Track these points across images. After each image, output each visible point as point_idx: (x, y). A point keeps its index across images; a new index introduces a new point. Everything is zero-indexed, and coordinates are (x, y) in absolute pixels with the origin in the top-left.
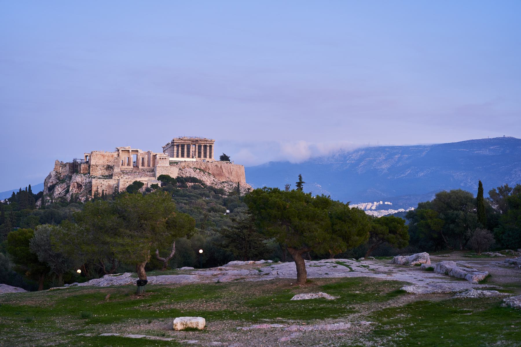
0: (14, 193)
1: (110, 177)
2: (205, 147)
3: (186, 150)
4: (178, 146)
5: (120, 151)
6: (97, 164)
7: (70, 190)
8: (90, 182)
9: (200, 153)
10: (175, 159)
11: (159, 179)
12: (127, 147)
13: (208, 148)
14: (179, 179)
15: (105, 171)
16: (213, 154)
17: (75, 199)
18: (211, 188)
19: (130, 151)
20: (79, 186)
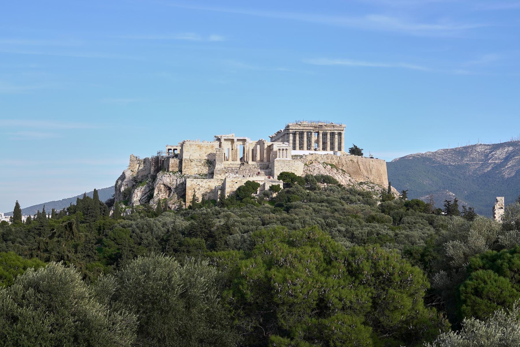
0: (78, 199)
2: (333, 134)
3: (305, 139)
4: (294, 134)
6: (191, 158)
7: (155, 195)
8: (184, 184)
9: (324, 143)
10: (298, 152)
12: (231, 135)
13: (336, 136)
15: (203, 167)
16: (343, 145)
17: (163, 207)
18: (352, 191)
19: (235, 140)
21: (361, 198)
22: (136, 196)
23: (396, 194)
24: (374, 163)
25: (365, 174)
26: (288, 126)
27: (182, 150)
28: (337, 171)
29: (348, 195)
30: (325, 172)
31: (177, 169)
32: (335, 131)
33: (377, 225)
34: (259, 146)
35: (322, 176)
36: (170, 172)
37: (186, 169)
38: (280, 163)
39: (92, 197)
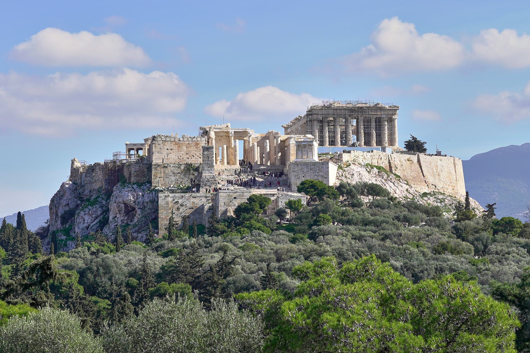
5: (212, 135)
7: (111, 218)
11: (299, 191)
20: (129, 210)
21: (424, 216)
22: (81, 220)
23: (478, 208)
25: (430, 179)
27: (150, 151)
29: (406, 213)
30: (370, 178)
33: (450, 257)
34: (268, 141)
38: (300, 167)
39: (15, 225)
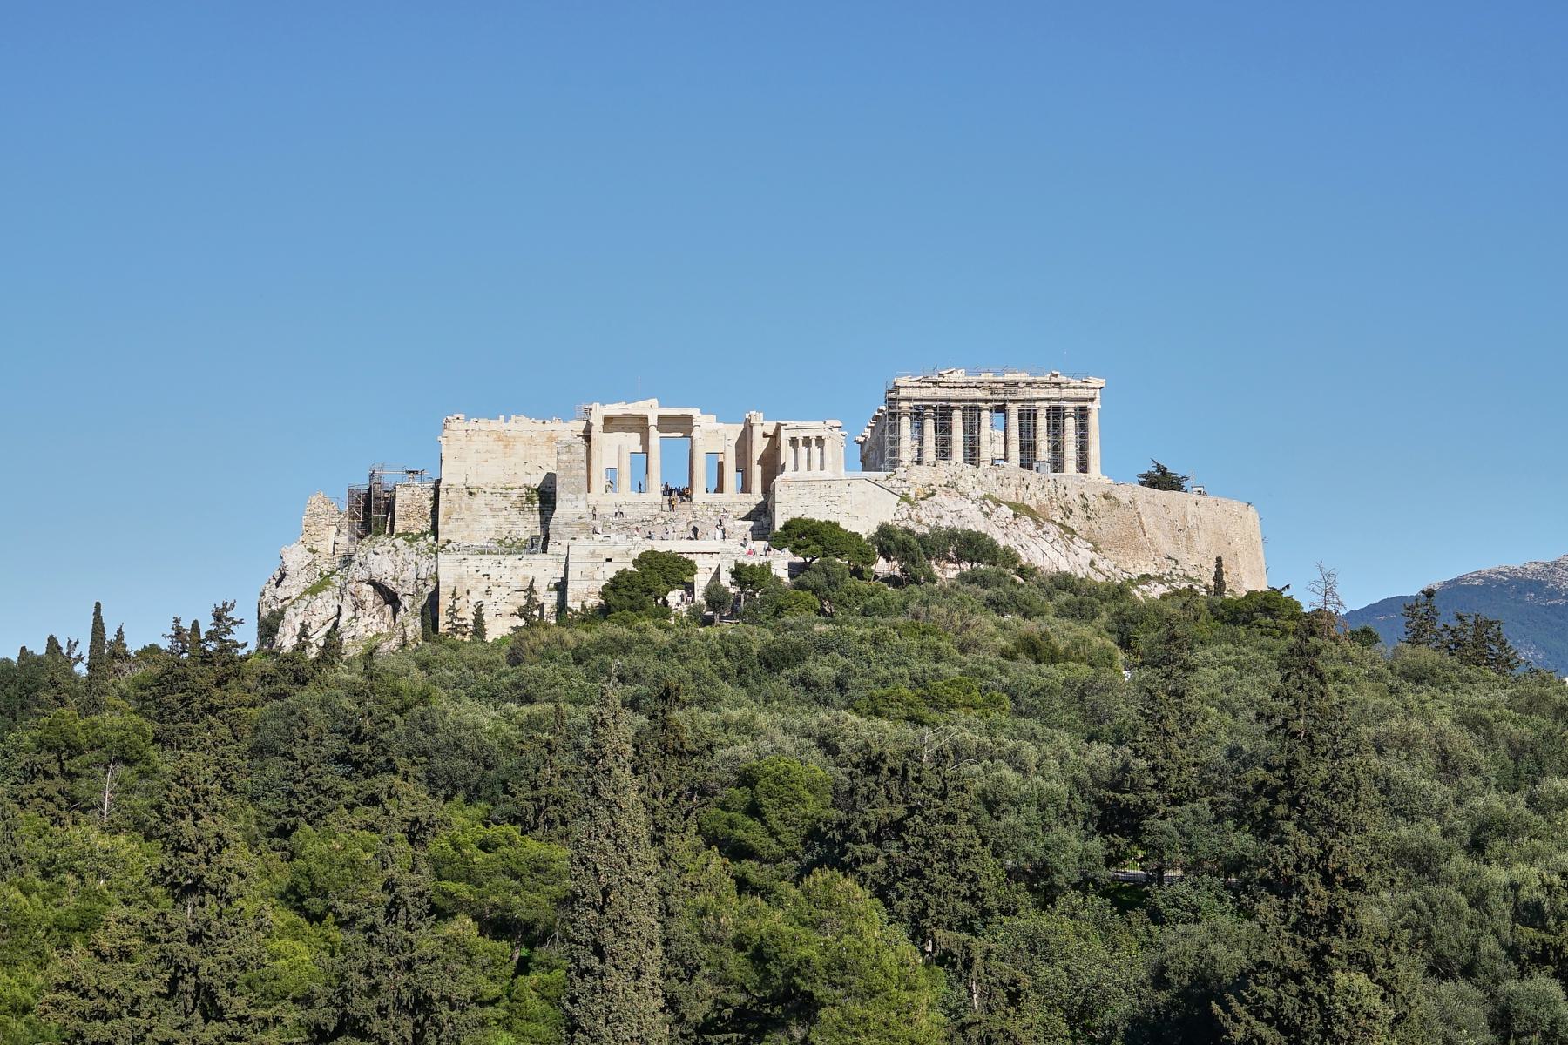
1: (541, 544)
2: (1056, 415)
3: (957, 434)
6: (473, 482)
9: (1028, 447)
13: (1070, 423)
14: (888, 541)
15: (514, 515)
19: (653, 421)
24: (1202, 511)
26: (896, 389)
28: (1039, 526)
31: (426, 525)
32: (1065, 404)
35: (952, 535)
36: (400, 535)
37: (452, 524)
38: (794, 492)
